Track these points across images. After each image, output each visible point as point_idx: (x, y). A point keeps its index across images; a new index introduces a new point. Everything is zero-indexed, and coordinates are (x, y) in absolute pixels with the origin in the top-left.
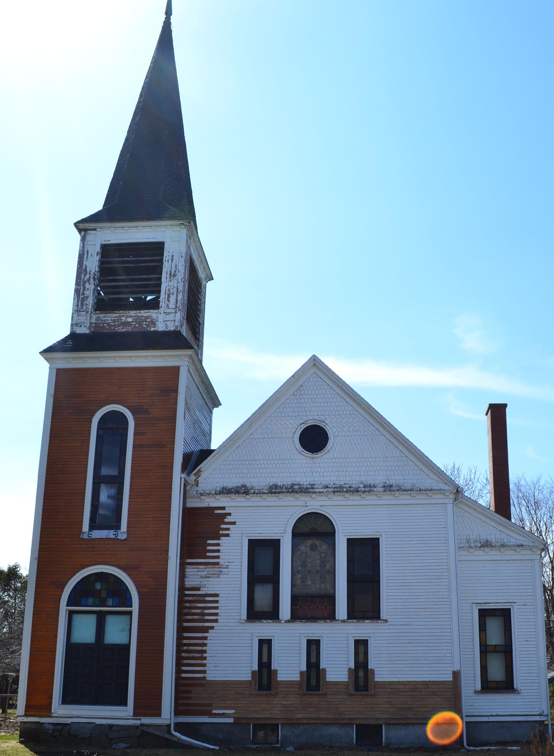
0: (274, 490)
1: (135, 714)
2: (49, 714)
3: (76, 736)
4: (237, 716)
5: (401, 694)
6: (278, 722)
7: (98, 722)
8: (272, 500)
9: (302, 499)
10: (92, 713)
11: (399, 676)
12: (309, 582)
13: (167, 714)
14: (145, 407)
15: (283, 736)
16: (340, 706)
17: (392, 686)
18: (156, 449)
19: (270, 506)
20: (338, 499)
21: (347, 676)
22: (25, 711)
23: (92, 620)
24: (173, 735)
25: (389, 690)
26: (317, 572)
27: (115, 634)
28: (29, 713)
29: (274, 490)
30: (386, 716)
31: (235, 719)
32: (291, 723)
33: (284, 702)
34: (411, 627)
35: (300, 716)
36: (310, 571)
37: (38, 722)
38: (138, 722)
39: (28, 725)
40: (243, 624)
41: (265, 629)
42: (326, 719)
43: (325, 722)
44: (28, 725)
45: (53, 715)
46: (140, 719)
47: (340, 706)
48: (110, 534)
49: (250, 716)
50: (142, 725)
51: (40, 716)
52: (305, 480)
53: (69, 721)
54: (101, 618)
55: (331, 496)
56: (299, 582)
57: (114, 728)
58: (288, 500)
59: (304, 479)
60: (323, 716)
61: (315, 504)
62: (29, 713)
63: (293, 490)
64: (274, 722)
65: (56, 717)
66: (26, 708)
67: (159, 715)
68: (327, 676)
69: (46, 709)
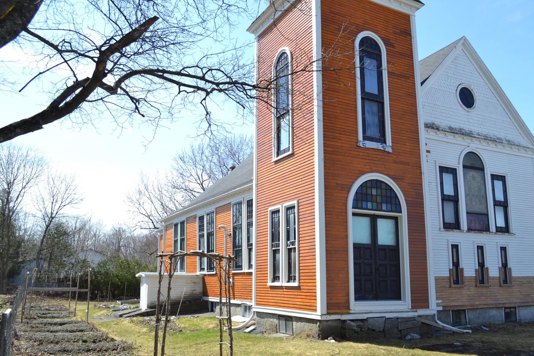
0: (453, 131)
1: (413, 307)
2: (348, 311)
3: (373, 330)
4: (445, 304)
5: (524, 285)
6: (465, 308)
7: (388, 316)
8: (450, 137)
9: (467, 141)
10: (369, 309)
11: (523, 273)
12: (474, 203)
13: (434, 306)
14: (391, 41)
15: (469, 319)
16: (497, 294)
17: (520, 280)
18: (403, 79)
19: (448, 143)
20: (492, 146)
21: (498, 273)
22: (328, 309)
23: (365, 222)
24: (437, 323)
25: (518, 283)
26: (477, 196)
27: (385, 237)
28: (330, 311)
29: (453, 131)
30: (518, 301)
31: (444, 307)
32: (474, 309)
33: (468, 293)
34: (524, 239)
35: (477, 303)
36: (473, 195)
37: (339, 320)
38: (416, 314)
39: (329, 323)
40: (442, 232)
41: (454, 237)
42: (491, 304)
43: (491, 306)
44: (330, 322)
45: (351, 312)
46: (416, 311)
47: (497, 294)
48: (378, 146)
49: (451, 305)
50: (420, 316)
51: (342, 314)
52: (467, 127)
53: (365, 317)
54: (374, 219)
55: (482, 141)
56: (468, 202)
57: (399, 320)
58: (459, 139)
59: (468, 127)
60: (489, 302)
61: (475, 146)
62: (330, 311)
63: (469, 134)
64: (463, 308)
65: (353, 313)
66: (327, 307)
67: (428, 307)
68: (513, 273)
69: (346, 307)
